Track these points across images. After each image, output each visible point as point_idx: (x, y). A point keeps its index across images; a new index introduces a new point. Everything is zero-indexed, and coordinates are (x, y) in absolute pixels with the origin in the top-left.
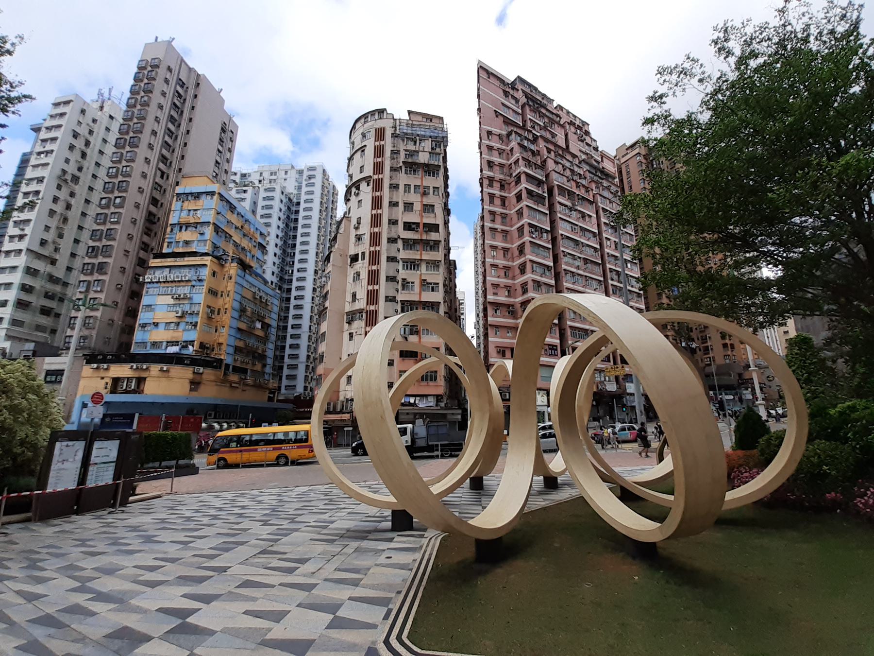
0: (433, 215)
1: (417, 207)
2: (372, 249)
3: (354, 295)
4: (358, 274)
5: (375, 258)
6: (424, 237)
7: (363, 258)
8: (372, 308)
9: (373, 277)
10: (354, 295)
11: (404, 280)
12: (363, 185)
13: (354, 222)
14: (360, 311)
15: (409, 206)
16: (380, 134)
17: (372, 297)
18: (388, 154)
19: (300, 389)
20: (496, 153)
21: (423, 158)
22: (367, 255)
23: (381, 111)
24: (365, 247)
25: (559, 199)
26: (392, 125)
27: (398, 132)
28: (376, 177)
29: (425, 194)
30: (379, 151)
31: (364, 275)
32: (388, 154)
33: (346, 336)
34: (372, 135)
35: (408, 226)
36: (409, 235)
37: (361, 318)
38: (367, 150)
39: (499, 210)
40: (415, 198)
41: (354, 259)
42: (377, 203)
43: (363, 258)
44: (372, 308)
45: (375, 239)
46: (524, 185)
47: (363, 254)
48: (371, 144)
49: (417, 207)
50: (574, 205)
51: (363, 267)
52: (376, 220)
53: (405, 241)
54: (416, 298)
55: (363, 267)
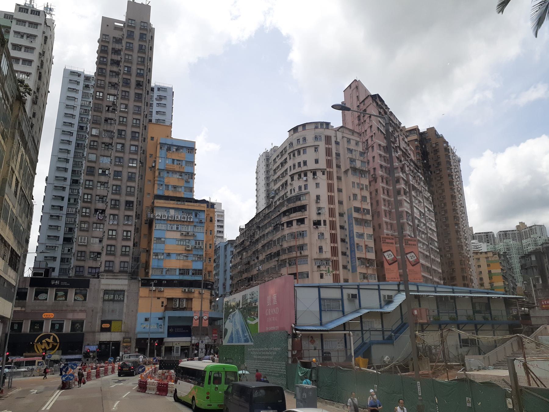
0: (366, 203)
1: (359, 197)
2: (331, 219)
3: (321, 249)
5: (333, 226)
6: (364, 218)
7: (325, 224)
8: (335, 258)
9: (333, 238)
10: (321, 249)
11: (357, 244)
12: (319, 174)
13: (314, 198)
14: (327, 260)
15: (355, 196)
16: (328, 139)
17: (334, 251)
18: (334, 155)
19: (178, 306)
20: (383, 159)
21: (358, 165)
22: (328, 222)
23: (328, 124)
24: (325, 216)
25: (413, 193)
26: (334, 135)
27: (338, 140)
28: (328, 170)
29: (362, 189)
30: (328, 152)
31: (327, 236)
32: (334, 155)
33: (317, 275)
34: (323, 138)
35: (357, 210)
36: (355, 215)
38: (319, 149)
39: (386, 197)
40: (357, 191)
41: (317, 224)
42: (330, 188)
43: (325, 224)
44: (335, 258)
45: (332, 212)
46: (402, 186)
47: (325, 221)
48: (322, 145)
49: (359, 197)
50: (417, 195)
51: (325, 229)
52: (331, 200)
53: (356, 219)
54: (363, 256)
55: (325, 229)
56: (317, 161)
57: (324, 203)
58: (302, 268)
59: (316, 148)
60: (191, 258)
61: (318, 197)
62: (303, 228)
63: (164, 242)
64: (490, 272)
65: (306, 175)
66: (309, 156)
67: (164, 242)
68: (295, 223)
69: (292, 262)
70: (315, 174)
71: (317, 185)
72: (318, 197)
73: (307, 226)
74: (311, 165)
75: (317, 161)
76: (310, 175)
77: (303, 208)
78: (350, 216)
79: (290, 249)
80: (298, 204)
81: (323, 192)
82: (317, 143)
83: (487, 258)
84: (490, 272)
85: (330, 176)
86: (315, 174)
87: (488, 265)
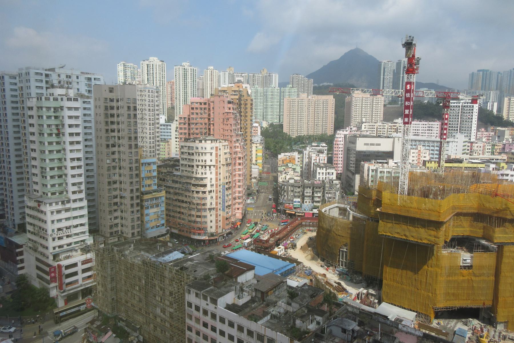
3: (211, 204)
4: (212, 197)
10: (211, 204)
12: (212, 167)
13: (209, 179)
14: (214, 209)
17: (217, 204)
24: (214, 188)
31: (214, 197)
34: (215, 148)
37: (214, 210)
41: (210, 192)
42: (217, 174)
48: (214, 151)
52: (217, 179)
55: (213, 194)
56: (211, 161)
57: (214, 182)
58: (204, 214)
59: (211, 155)
60: (160, 219)
61: (211, 179)
62: (204, 196)
63: (149, 215)
64: (256, 154)
65: (205, 167)
66: (208, 157)
67: (149, 215)
68: (201, 193)
69: (199, 210)
70: (210, 167)
71: (211, 173)
72: (211, 179)
73: (207, 195)
74: (208, 163)
75: (211, 161)
76: (208, 168)
77: (205, 186)
78: (224, 186)
79: (198, 204)
80: (201, 183)
81: (213, 176)
82: (211, 151)
83: (256, 147)
84: (256, 154)
85: (217, 169)
86: (210, 167)
87: (256, 151)
